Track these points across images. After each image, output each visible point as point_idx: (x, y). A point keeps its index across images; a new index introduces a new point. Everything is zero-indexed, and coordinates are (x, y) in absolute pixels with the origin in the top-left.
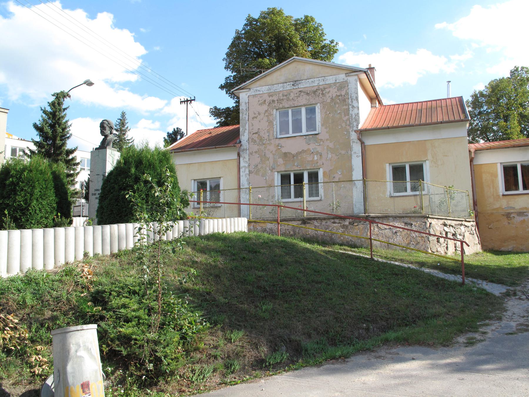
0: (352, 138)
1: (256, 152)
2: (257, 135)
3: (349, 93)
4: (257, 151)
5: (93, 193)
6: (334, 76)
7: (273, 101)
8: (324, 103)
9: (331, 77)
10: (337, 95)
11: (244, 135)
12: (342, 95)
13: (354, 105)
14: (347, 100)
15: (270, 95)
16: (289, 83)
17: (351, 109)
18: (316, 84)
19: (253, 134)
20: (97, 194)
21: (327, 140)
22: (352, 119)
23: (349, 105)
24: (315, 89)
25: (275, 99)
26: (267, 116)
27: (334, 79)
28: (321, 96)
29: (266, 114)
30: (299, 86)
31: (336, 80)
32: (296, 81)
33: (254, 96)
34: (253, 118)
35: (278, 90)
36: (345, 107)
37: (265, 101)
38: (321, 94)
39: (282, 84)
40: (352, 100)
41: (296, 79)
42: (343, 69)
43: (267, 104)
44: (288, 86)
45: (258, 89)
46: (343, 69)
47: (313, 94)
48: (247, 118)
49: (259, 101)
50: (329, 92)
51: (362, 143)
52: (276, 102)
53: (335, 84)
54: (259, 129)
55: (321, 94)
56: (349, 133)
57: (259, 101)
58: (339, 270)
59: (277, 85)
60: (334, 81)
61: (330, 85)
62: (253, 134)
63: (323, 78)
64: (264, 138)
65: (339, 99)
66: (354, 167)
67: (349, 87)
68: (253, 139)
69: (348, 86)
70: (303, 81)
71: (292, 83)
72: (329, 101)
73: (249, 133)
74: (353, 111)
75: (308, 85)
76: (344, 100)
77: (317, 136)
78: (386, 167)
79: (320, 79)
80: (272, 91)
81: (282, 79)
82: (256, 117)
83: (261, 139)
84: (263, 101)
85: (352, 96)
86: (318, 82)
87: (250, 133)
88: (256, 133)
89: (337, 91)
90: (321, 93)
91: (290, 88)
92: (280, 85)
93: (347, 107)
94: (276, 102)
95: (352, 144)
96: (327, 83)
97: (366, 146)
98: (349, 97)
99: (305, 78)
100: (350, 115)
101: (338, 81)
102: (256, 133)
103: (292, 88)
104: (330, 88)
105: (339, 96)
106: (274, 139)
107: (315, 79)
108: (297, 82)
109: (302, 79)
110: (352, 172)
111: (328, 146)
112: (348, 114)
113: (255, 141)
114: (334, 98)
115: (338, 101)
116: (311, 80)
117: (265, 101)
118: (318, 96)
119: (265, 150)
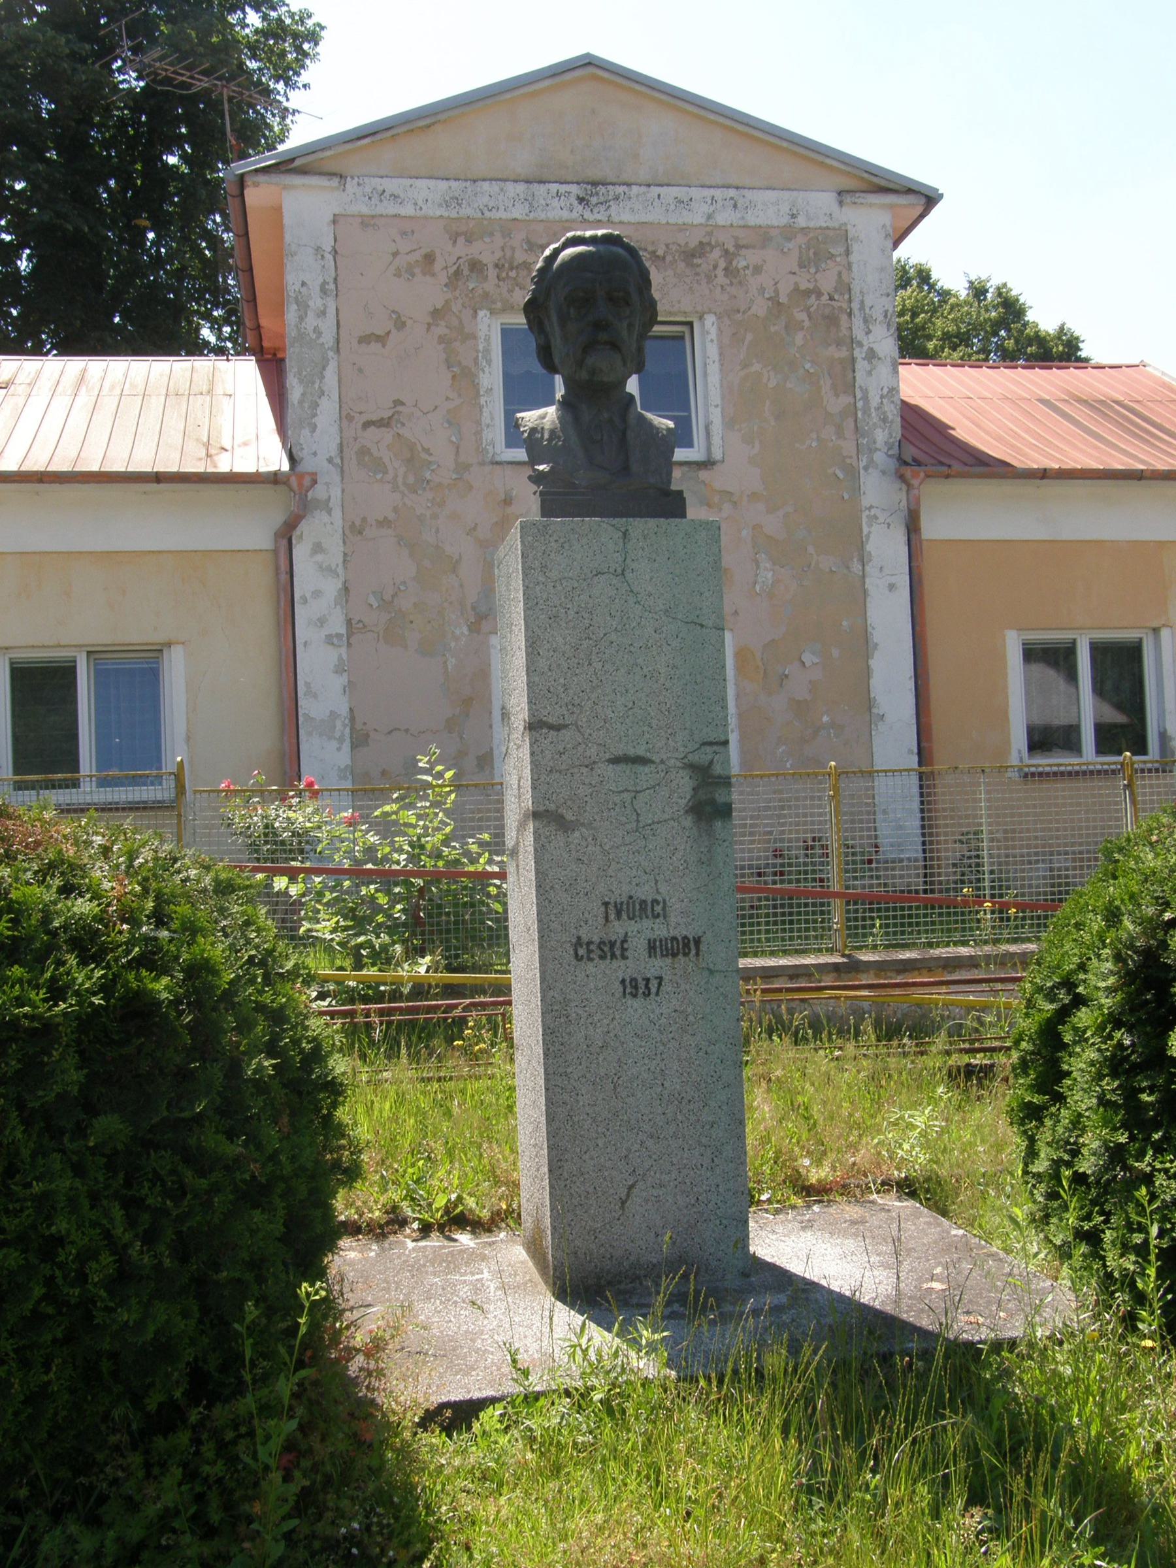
0: (865, 502)
1: (384, 523)
2: (387, 435)
3: (856, 289)
4: (391, 516)
5: (593, 932)
6: (786, 195)
7: (476, 267)
8: (739, 316)
9: (771, 195)
10: (796, 289)
11: (314, 428)
12: (819, 294)
13: (875, 347)
14: (844, 317)
15: (460, 232)
16: (563, 188)
17: (861, 365)
18: (699, 219)
19: (367, 425)
20: (638, 945)
21: (754, 496)
22: (866, 410)
23: (852, 342)
24: (693, 244)
25: (488, 259)
26: (441, 339)
27: (785, 209)
28: (721, 279)
29: (441, 330)
30: (613, 210)
31: (793, 216)
32: (595, 184)
33: (367, 222)
34: (365, 340)
35: (501, 214)
36: (834, 353)
37: (429, 258)
38: (720, 272)
39: (521, 187)
40: (866, 321)
41: (594, 173)
42: (831, 168)
43: (443, 278)
44: (555, 203)
45: (391, 185)
46: (831, 168)
47: (682, 265)
48: (328, 338)
49: (395, 254)
50: (758, 270)
51: (912, 526)
52: (492, 273)
53: (789, 232)
54: (398, 403)
55: (720, 272)
56: (853, 474)
57: (395, 254)
58: (984, 1175)
59: (495, 187)
60: (785, 220)
61: (763, 236)
62: (367, 425)
63: (732, 193)
64: (427, 451)
65: (807, 309)
66: (877, 636)
67: (854, 258)
68: (364, 452)
69: (848, 252)
70: (635, 189)
71: (574, 189)
72: (760, 308)
73: (345, 417)
74: (870, 373)
75: (655, 215)
76: (832, 320)
77: (703, 475)
78: (1004, 646)
79: (718, 193)
80: (466, 211)
81: (523, 160)
82: (381, 339)
83: (414, 457)
84: (417, 256)
85: (868, 303)
86: (706, 209)
87: (350, 418)
88: (382, 423)
89: (796, 269)
90: (722, 264)
91: (565, 214)
92: (510, 186)
93: (844, 353)
94: (492, 273)
95: (865, 530)
96: (752, 220)
97: (924, 543)
98: (855, 306)
99: (644, 175)
100: (859, 395)
101: (801, 222)
102: (382, 423)
103: (574, 215)
104: (763, 247)
105: (807, 293)
106: (482, 464)
107: (695, 193)
108: (602, 189)
109: (625, 177)
110: (868, 657)
111: (757, 527)
112: (850, 387)
113: (379, 466)
114: (783, 299)
115: (803, 316)
116: (674, 191)
117: (429, 258)
118: (710, 279)
119: (435, 516)
